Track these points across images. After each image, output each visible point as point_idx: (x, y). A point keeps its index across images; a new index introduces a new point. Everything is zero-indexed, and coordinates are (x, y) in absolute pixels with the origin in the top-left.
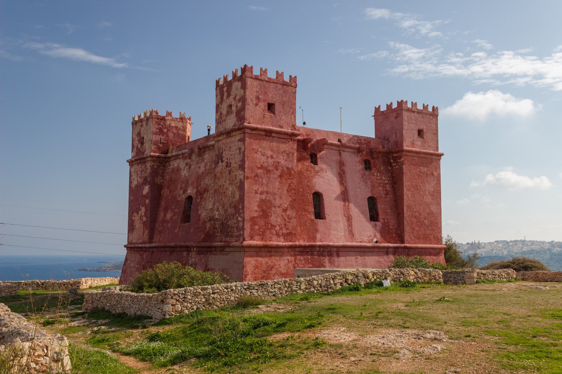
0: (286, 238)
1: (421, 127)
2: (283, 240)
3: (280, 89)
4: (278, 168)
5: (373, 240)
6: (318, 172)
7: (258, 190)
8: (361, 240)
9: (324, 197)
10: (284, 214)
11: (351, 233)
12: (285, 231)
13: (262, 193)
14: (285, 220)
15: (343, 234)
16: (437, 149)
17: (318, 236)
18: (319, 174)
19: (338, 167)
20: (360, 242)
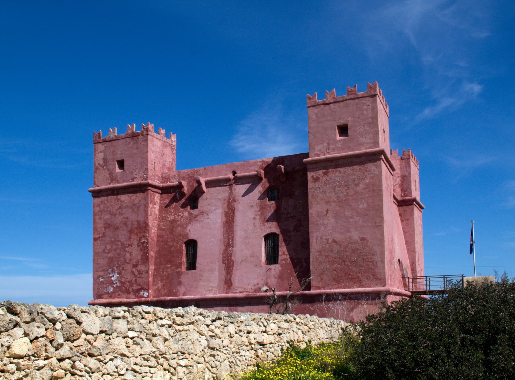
0: (137, 294)
1: (342, 122)
2: (133, 297)
3: (129, 143)
4: (128, 223)
5: (260, 289)
6: (196, 216)
7: (106, 248)
8: (241, 290)
9: (199, 245)
10: (134, 270)
11: (228, 283)
12: (135, 287)
13: (110, 251)
14: (135, 276)
15: (216, 285)
16: (376, 143)
17: (182, 289)
18: (196, 219)
19: (226, 206)
20: (240, 292)
